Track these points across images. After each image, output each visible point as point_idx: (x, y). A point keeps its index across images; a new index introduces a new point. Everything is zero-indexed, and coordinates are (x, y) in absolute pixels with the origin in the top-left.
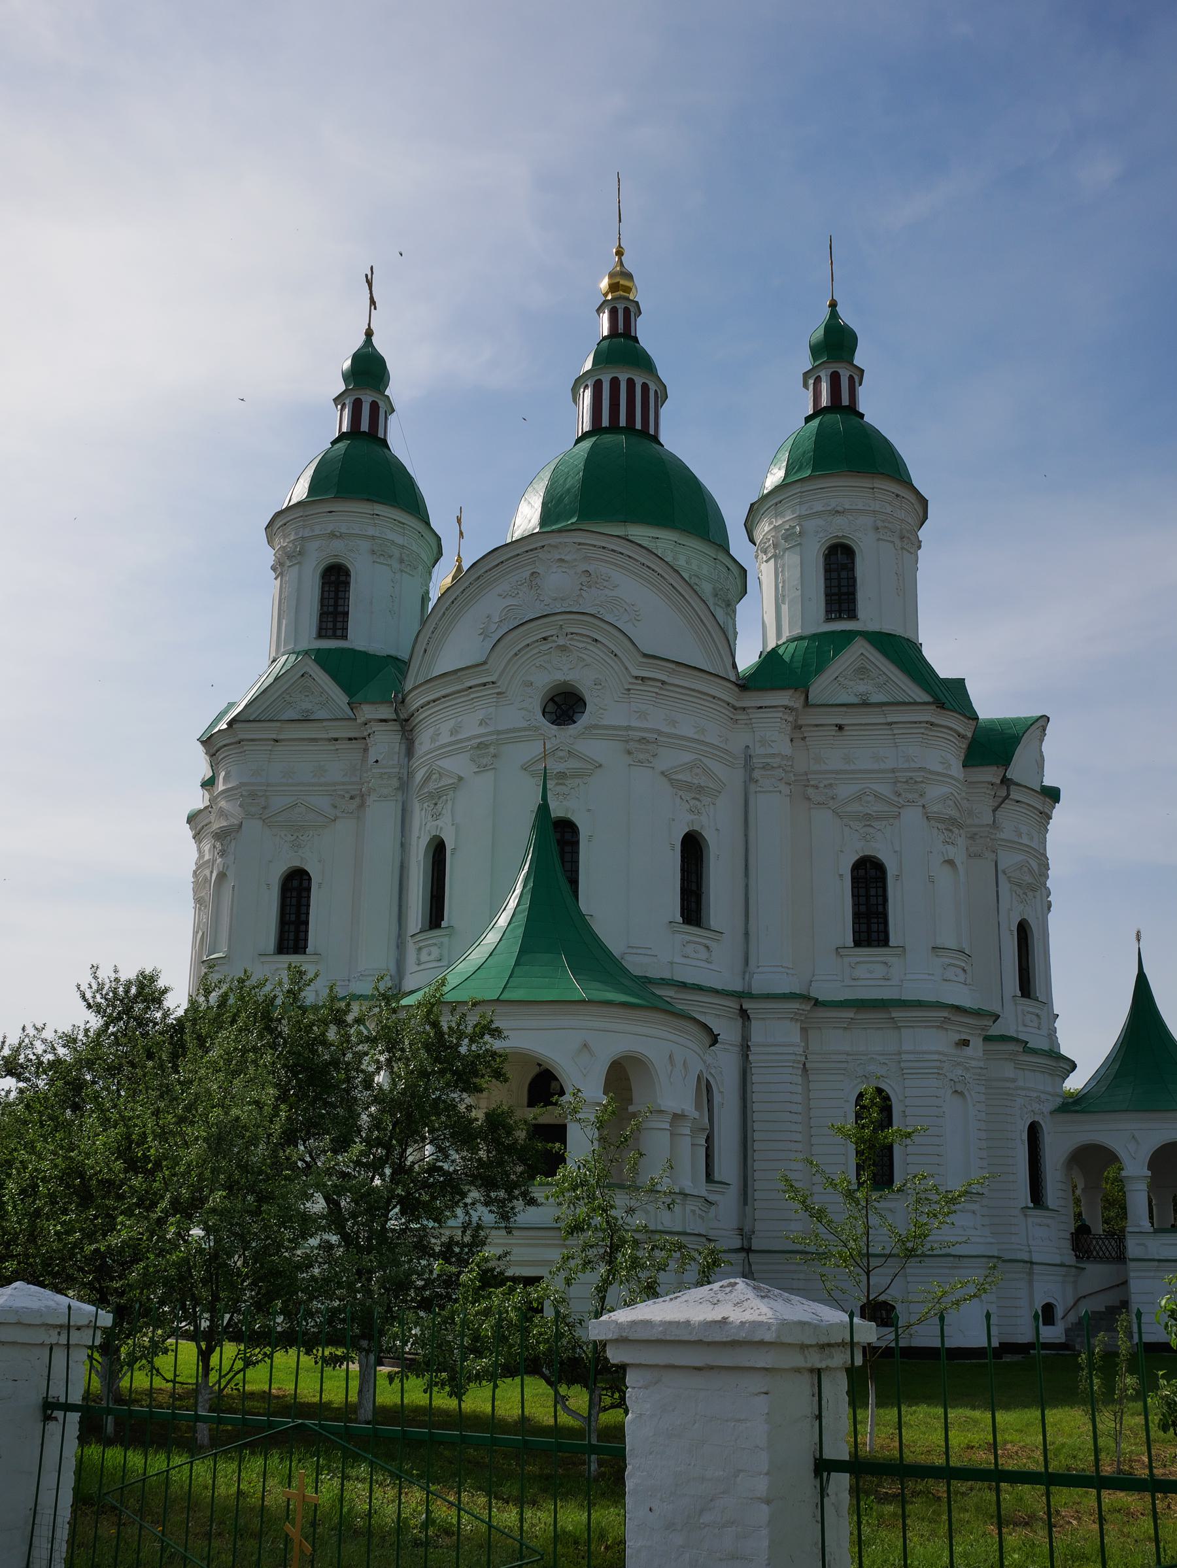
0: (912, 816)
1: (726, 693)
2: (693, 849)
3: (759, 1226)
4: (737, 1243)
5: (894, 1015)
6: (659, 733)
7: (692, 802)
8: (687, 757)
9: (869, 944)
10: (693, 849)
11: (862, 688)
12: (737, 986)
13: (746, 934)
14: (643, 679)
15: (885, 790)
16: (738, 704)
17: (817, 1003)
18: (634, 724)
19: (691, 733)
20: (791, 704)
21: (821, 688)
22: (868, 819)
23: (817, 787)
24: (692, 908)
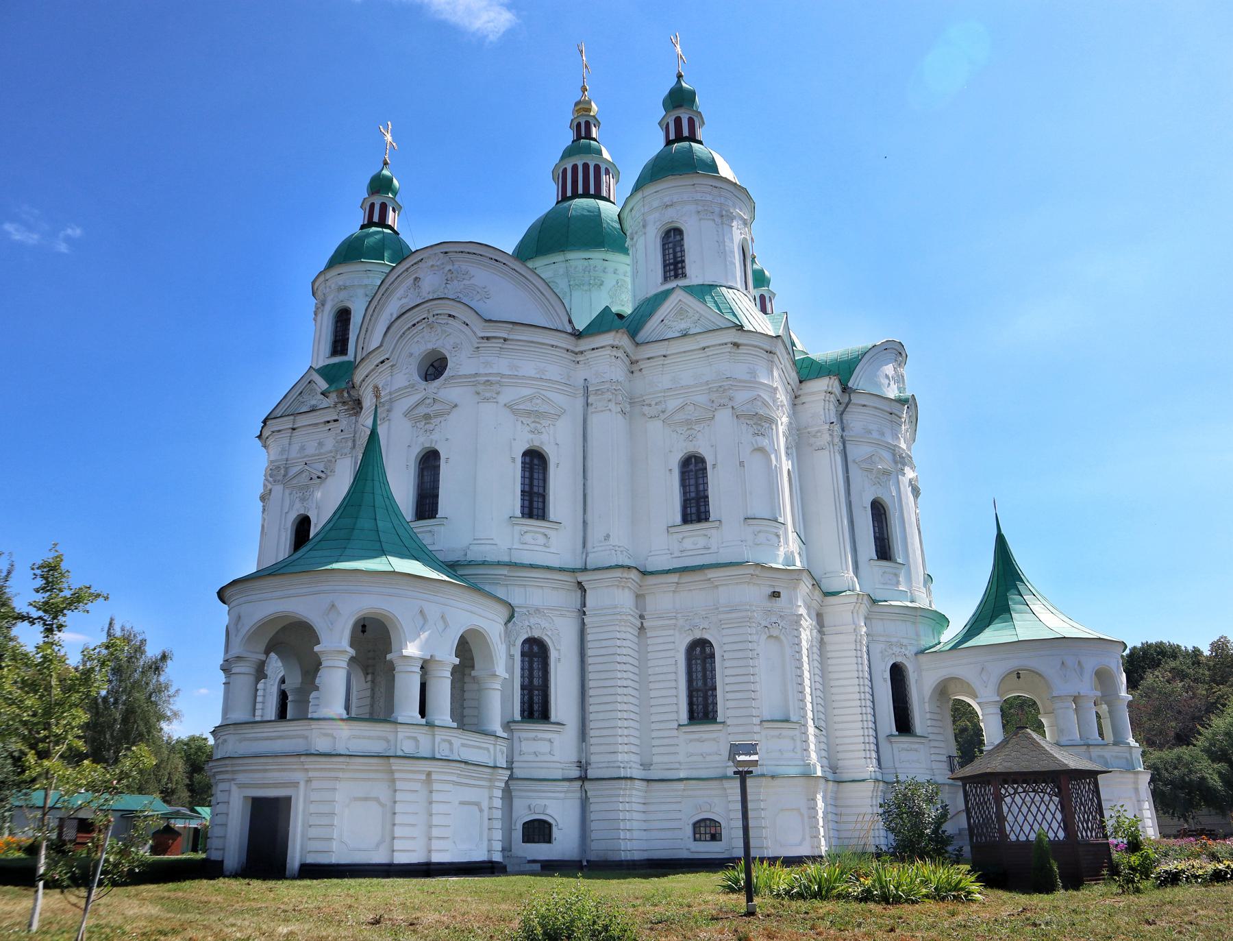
0: (724, 417)
1: (565, 342)
2: (535, 462)
3: (593, 759)
4: (575, 773)
5: (709, 576)
6: (503, 376)
7: (533, 425)
8: (527, 392)
9: (691, 522)
10: (535, 462)
11: (683, 325)
12: (579, 565)
13: (584, 522)
14: (488, 338)
15: (702, 399)
16: (577, 350)
17: (644, 573)
18: (482, 371)
19: (532, 373)
20: (616, 343)
21: (652, 327)
22: (688, 422)
23: (650, 405)
24: (534, 503)
